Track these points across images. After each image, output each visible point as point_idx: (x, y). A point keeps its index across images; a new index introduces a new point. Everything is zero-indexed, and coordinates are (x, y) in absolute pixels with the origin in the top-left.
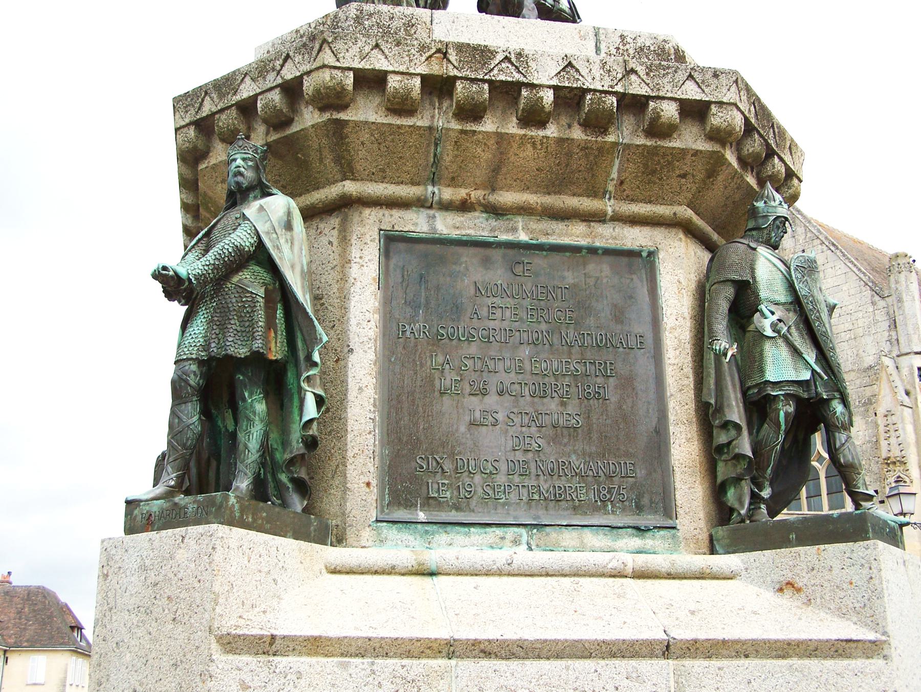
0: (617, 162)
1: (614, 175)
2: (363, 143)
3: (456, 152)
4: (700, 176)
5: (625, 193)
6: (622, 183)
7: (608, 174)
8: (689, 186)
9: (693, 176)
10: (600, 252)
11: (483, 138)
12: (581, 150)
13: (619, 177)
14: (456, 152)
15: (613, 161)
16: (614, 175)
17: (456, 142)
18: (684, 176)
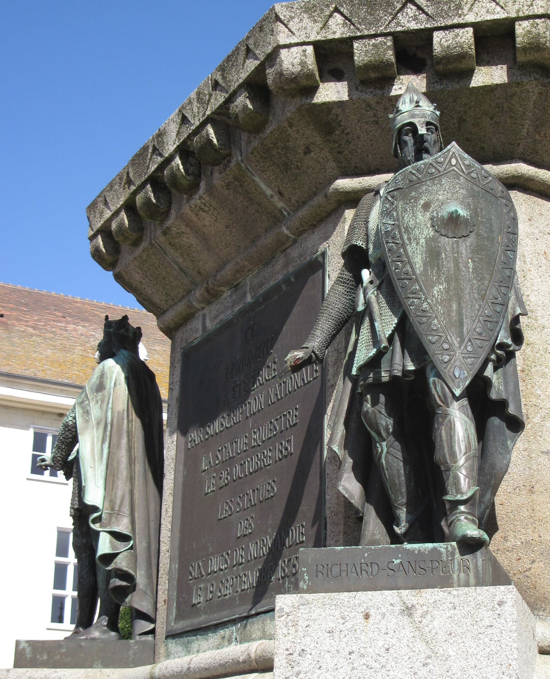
0: (257, 179)
1: (269, 192)
2: (141, 282)
3: (179, 252)
4: (319, 140)
5: (293, 201)
6: (281, 193)
7: (266, 196)
8: (322, 155)
9: (312, 143)
10: (292, 279)
11: (178, 229)
12: (228, 189)
13: (273, 190)
14: (179, 252)
15: (254, 181)
16: (269, 192)
17: (170, 244)
18: (308, 151)
